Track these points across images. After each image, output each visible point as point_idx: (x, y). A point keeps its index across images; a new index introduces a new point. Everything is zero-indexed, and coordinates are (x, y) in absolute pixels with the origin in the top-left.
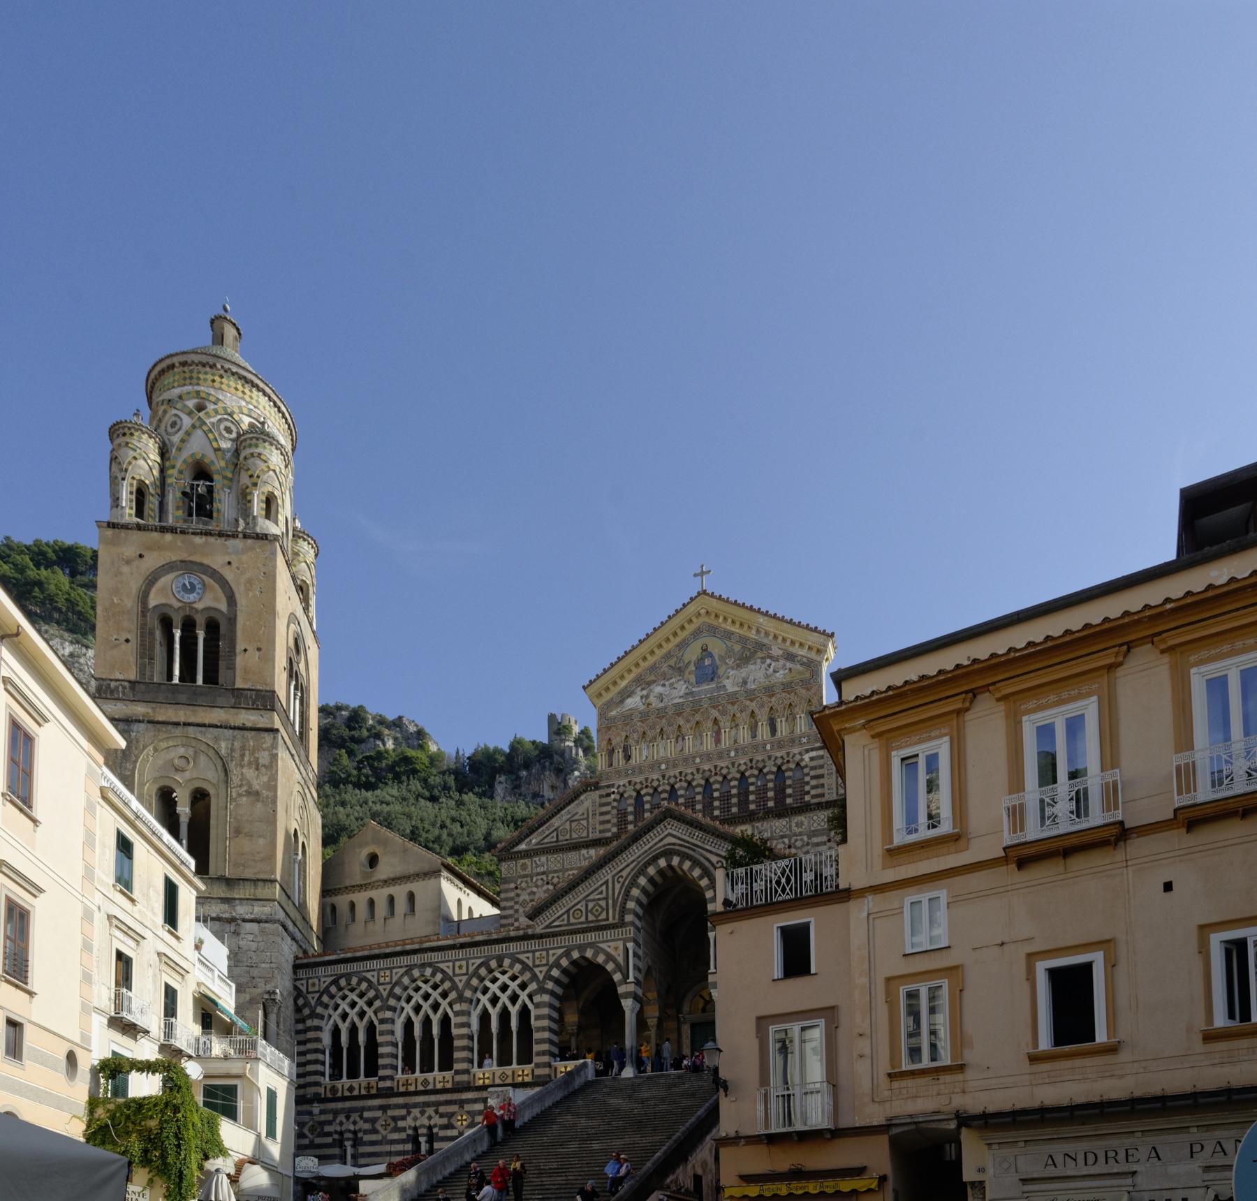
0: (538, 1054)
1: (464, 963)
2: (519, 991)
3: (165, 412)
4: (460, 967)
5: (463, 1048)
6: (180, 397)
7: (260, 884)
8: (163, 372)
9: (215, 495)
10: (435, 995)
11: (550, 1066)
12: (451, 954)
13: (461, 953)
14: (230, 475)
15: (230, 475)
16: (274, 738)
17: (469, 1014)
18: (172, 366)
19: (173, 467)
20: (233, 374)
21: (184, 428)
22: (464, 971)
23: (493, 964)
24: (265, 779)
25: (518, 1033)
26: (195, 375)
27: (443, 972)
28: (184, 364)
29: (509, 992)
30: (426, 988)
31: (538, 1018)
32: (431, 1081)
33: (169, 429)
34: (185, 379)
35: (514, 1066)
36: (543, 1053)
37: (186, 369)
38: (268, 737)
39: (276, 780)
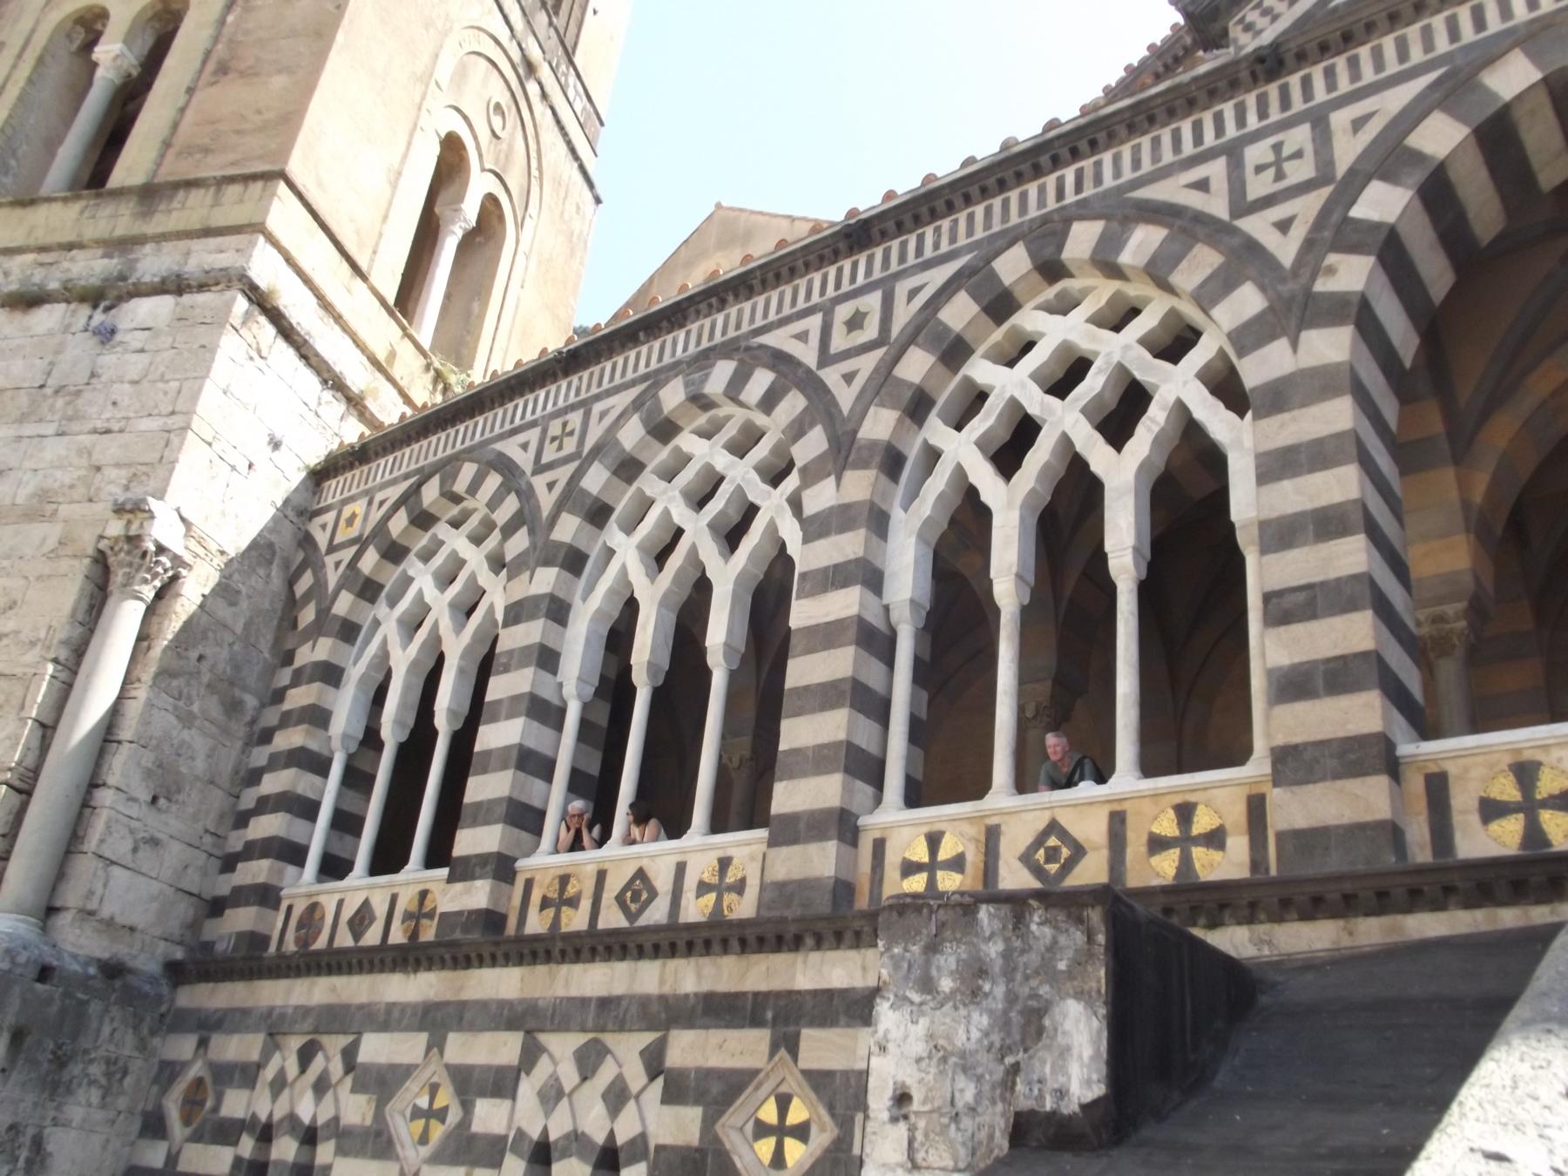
0: (1296, 685)
1: (873, 301)
2: (1148, 369)
4: (855, 323)
5: (825, 696)
7: (233, 191)
10: (742, 474)
11: (1393, 767)
12: (816, 285)
13: (861, 267)
17: (879, 522)
22: (871, 331)
23: (1013, 265)
25: (1147, 591)
27: (779, 360)
29: (1093, 384)
30: (704, 452)
31: (1277, 466)
32: (662, 881)
35: (1126, 779)
36: (1336, 676)
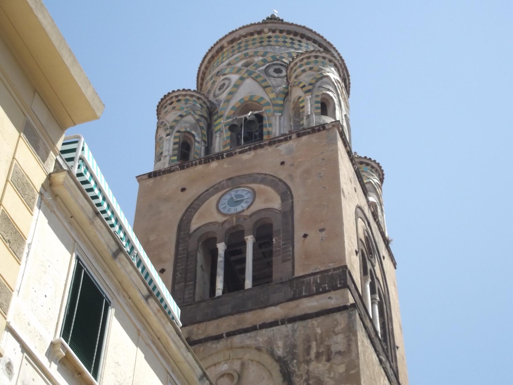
3: (214, 83)
6: (229, 64)
8: (213, 57)
9: (266, 122)
14: (281, 102)
15: (281, 102)
16: (350, 316)
18: (222, 48)
19: (221, 116)
20: (281, 32)
21: (232, 84)
24: (342, 369)
26: (243, 45)
28: (232, 41)
33: (218, 92)
34: (233, 51)
37: (234, 44)
38: (338, 316)
39: (357, 366)
